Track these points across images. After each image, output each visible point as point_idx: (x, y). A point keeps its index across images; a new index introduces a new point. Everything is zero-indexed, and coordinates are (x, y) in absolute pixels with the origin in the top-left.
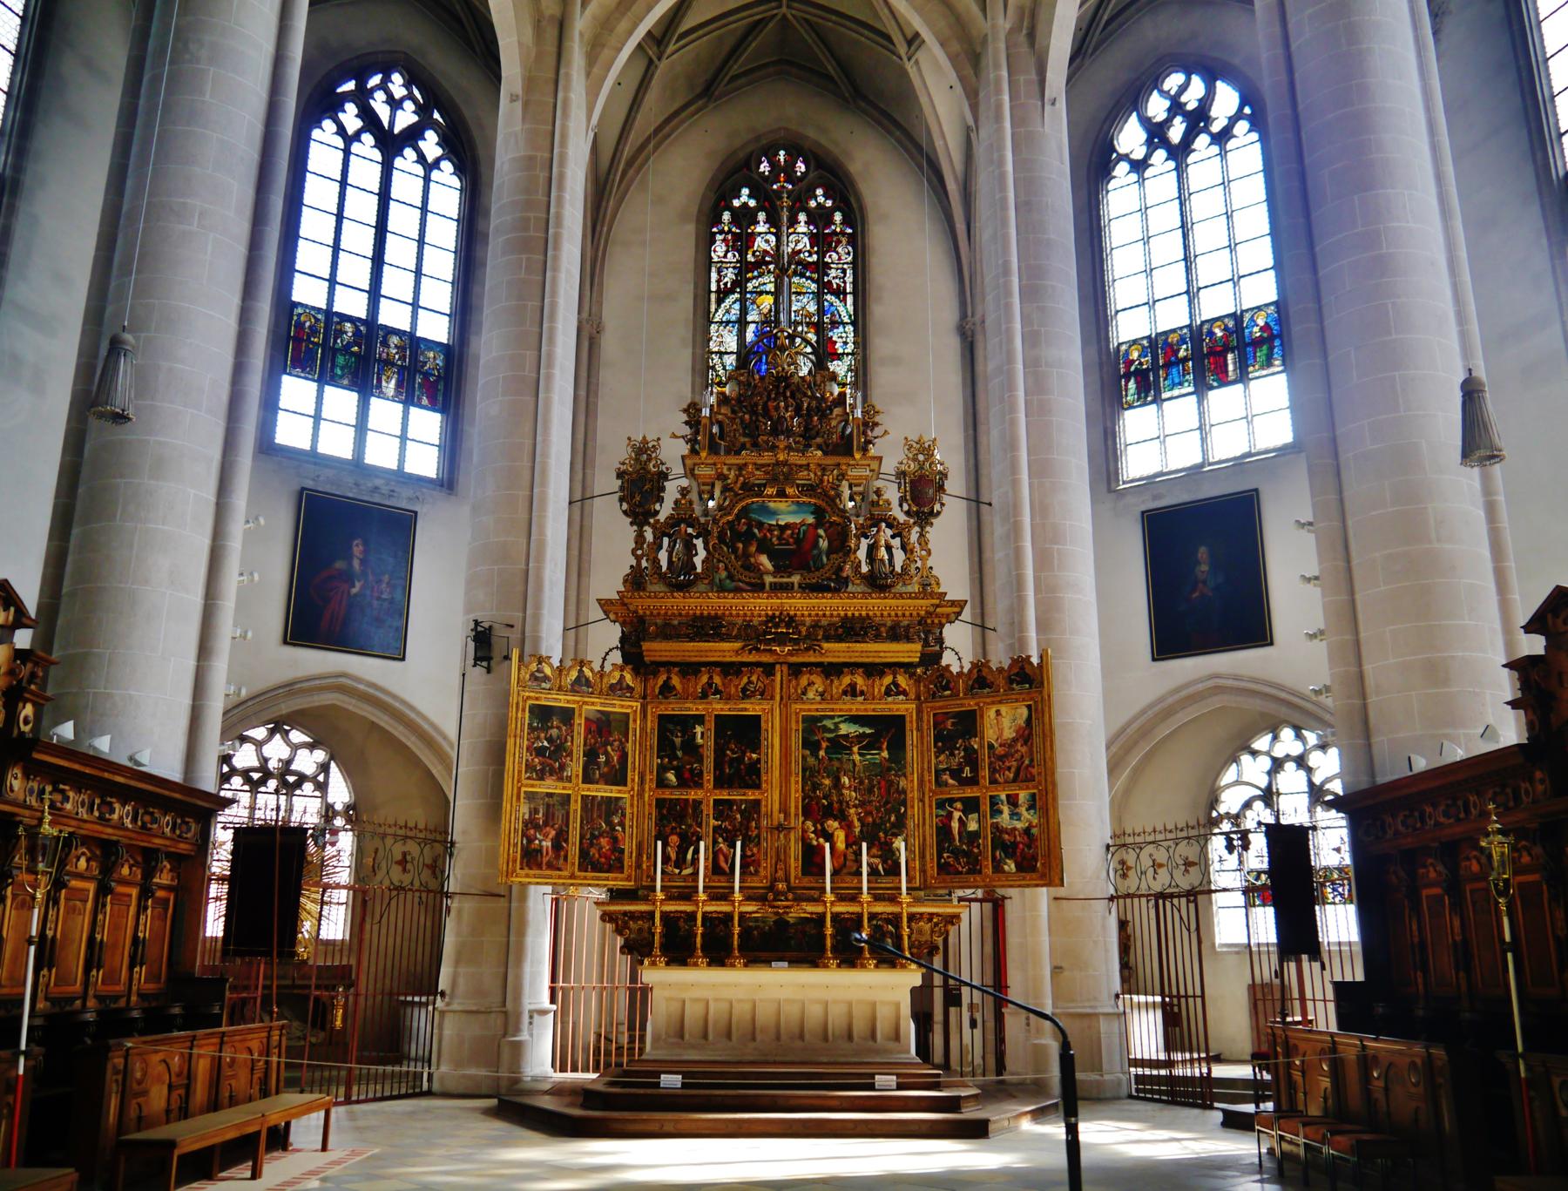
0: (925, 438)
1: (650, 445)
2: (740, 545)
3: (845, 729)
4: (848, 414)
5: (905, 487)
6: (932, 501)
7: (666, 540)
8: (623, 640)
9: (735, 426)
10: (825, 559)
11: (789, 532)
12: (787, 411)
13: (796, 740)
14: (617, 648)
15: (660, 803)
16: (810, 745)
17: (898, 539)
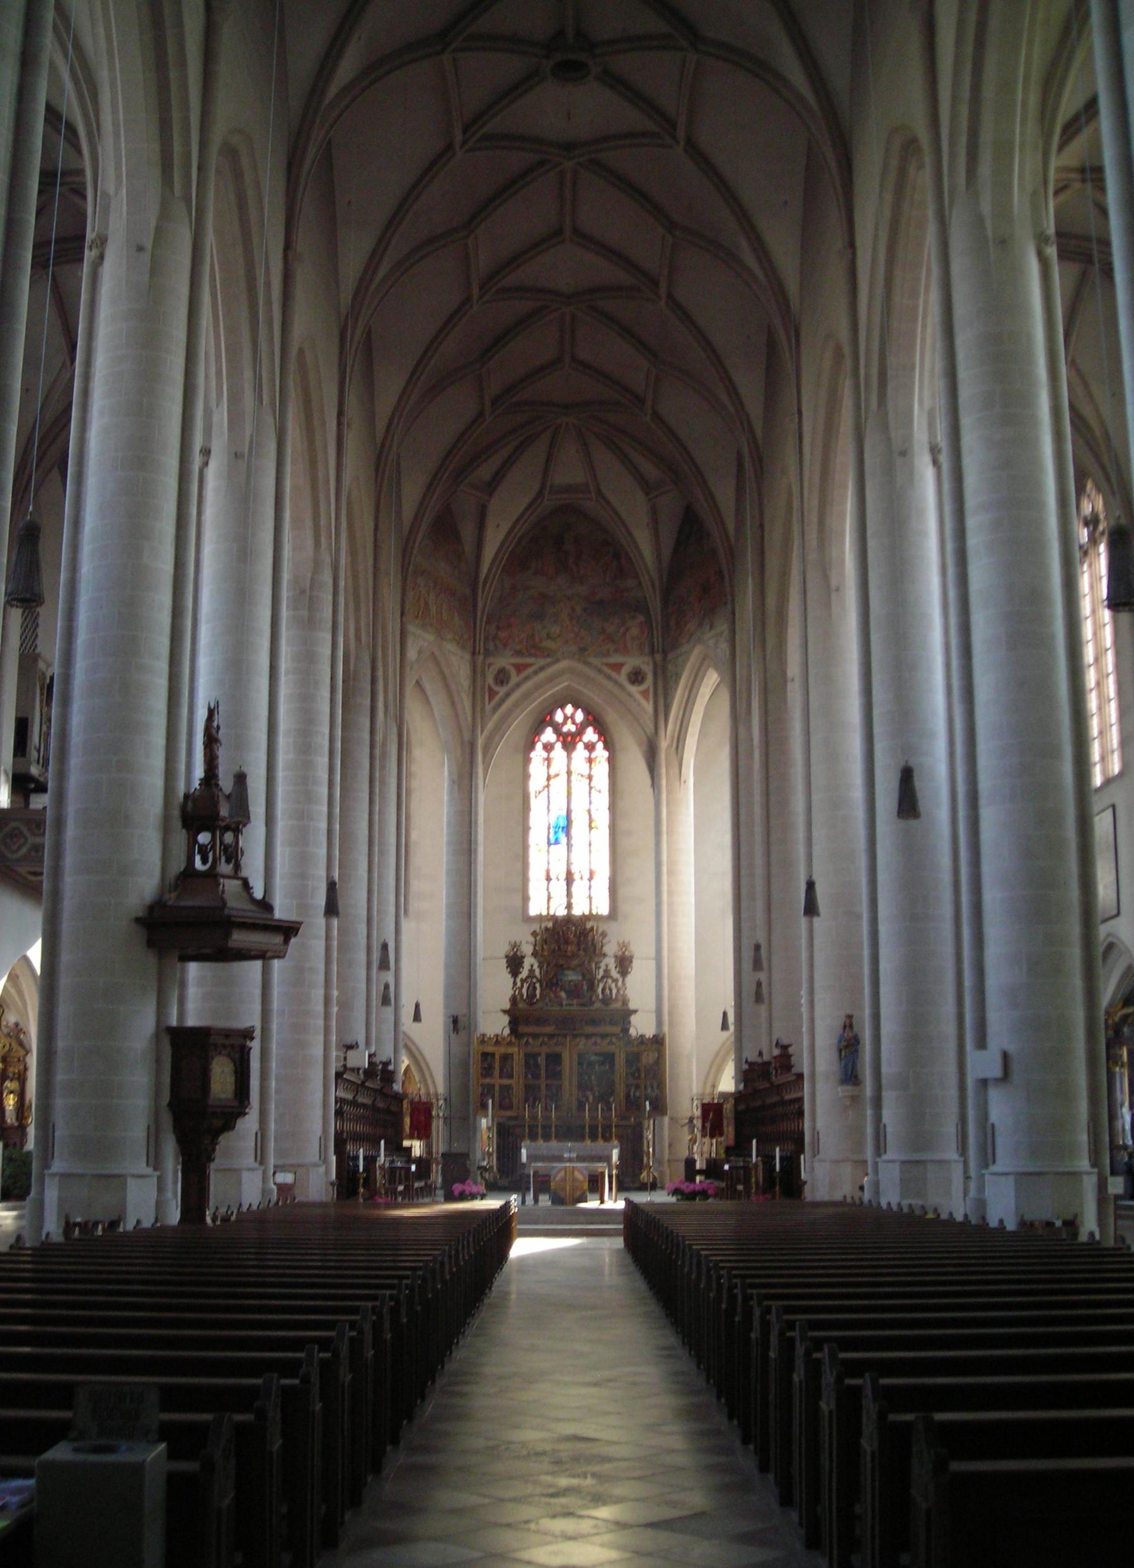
2: (554, 989)
3: (593, 1058)
8: (510, 1022)
13: (575, 1063)
15: (526, 1086)
16: (580, 1064)
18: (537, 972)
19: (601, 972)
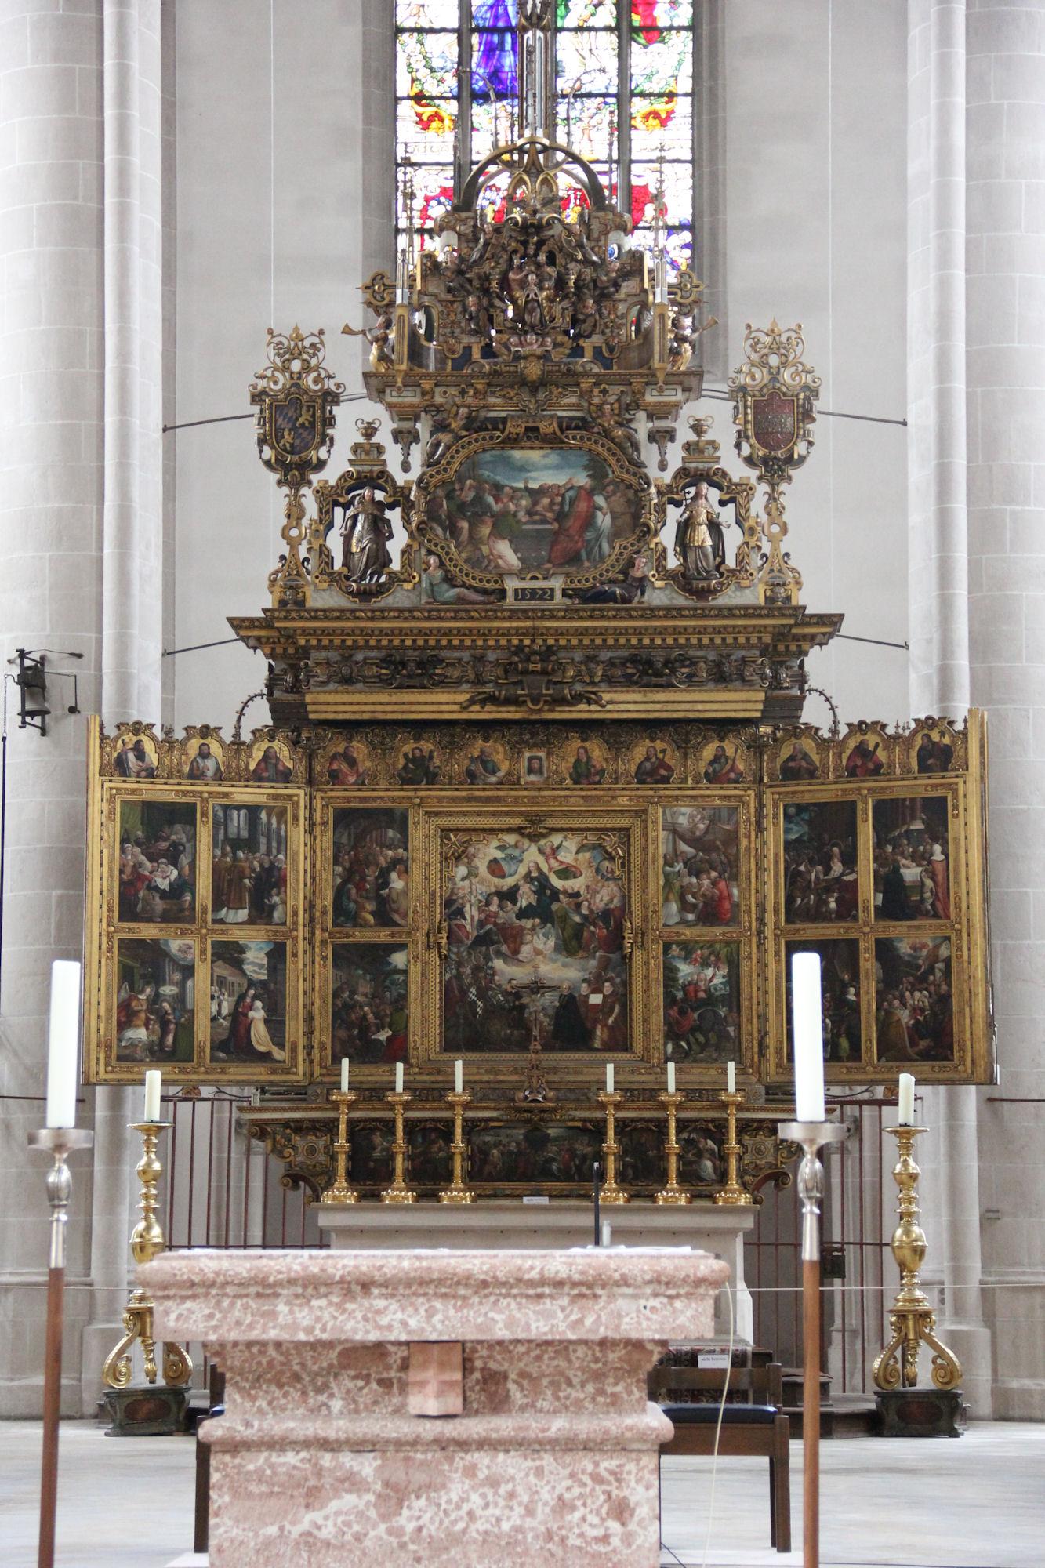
0: (782, 326)
1: (307, 343)
2: (464, 525)
4: (645, 291)
5: (746, 414)
6: (791, 438)
7: (338, 512)
8: (272, 683)
9: (452, 317)
10: (605, 547)
11: (546, 501)
12: (541, 289)
14: (262, 695)
17: (731, 507)
18: (393, 456)
19: (675, 456)
